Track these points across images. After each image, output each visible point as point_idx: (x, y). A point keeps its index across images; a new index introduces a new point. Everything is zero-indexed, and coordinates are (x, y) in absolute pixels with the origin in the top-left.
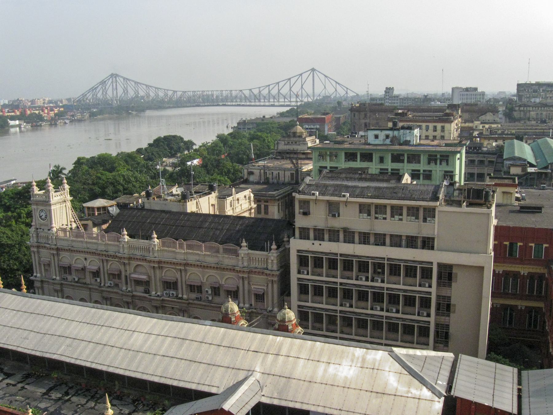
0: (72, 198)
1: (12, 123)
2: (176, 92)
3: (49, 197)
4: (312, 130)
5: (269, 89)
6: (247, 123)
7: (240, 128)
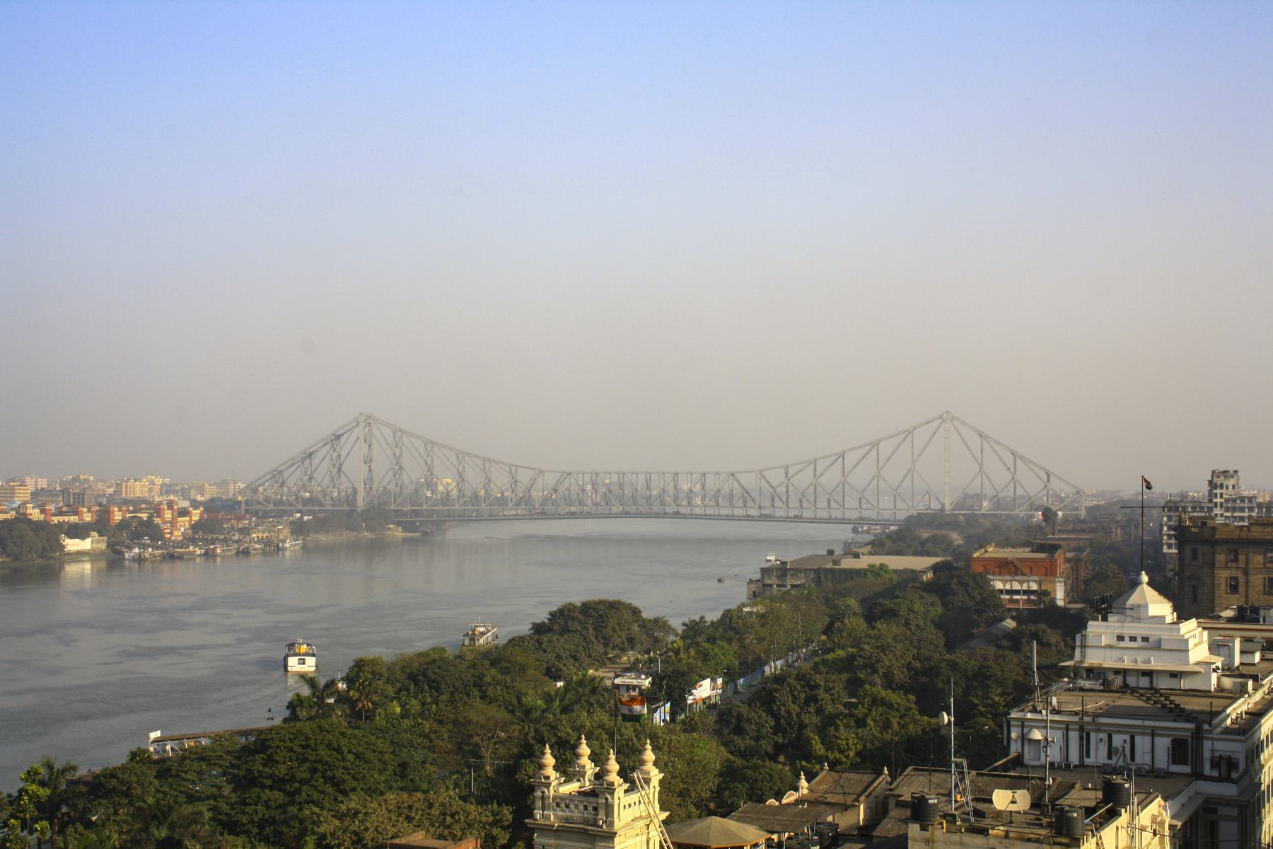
0: (664, 815)
1: (72, 545)
2: (542, 472)
3: (609, 809)
4: (1015, 597)
5: (815, 470)
6: (790, 569)
7: (771, 586)
